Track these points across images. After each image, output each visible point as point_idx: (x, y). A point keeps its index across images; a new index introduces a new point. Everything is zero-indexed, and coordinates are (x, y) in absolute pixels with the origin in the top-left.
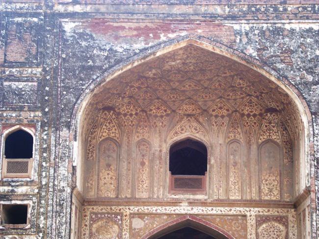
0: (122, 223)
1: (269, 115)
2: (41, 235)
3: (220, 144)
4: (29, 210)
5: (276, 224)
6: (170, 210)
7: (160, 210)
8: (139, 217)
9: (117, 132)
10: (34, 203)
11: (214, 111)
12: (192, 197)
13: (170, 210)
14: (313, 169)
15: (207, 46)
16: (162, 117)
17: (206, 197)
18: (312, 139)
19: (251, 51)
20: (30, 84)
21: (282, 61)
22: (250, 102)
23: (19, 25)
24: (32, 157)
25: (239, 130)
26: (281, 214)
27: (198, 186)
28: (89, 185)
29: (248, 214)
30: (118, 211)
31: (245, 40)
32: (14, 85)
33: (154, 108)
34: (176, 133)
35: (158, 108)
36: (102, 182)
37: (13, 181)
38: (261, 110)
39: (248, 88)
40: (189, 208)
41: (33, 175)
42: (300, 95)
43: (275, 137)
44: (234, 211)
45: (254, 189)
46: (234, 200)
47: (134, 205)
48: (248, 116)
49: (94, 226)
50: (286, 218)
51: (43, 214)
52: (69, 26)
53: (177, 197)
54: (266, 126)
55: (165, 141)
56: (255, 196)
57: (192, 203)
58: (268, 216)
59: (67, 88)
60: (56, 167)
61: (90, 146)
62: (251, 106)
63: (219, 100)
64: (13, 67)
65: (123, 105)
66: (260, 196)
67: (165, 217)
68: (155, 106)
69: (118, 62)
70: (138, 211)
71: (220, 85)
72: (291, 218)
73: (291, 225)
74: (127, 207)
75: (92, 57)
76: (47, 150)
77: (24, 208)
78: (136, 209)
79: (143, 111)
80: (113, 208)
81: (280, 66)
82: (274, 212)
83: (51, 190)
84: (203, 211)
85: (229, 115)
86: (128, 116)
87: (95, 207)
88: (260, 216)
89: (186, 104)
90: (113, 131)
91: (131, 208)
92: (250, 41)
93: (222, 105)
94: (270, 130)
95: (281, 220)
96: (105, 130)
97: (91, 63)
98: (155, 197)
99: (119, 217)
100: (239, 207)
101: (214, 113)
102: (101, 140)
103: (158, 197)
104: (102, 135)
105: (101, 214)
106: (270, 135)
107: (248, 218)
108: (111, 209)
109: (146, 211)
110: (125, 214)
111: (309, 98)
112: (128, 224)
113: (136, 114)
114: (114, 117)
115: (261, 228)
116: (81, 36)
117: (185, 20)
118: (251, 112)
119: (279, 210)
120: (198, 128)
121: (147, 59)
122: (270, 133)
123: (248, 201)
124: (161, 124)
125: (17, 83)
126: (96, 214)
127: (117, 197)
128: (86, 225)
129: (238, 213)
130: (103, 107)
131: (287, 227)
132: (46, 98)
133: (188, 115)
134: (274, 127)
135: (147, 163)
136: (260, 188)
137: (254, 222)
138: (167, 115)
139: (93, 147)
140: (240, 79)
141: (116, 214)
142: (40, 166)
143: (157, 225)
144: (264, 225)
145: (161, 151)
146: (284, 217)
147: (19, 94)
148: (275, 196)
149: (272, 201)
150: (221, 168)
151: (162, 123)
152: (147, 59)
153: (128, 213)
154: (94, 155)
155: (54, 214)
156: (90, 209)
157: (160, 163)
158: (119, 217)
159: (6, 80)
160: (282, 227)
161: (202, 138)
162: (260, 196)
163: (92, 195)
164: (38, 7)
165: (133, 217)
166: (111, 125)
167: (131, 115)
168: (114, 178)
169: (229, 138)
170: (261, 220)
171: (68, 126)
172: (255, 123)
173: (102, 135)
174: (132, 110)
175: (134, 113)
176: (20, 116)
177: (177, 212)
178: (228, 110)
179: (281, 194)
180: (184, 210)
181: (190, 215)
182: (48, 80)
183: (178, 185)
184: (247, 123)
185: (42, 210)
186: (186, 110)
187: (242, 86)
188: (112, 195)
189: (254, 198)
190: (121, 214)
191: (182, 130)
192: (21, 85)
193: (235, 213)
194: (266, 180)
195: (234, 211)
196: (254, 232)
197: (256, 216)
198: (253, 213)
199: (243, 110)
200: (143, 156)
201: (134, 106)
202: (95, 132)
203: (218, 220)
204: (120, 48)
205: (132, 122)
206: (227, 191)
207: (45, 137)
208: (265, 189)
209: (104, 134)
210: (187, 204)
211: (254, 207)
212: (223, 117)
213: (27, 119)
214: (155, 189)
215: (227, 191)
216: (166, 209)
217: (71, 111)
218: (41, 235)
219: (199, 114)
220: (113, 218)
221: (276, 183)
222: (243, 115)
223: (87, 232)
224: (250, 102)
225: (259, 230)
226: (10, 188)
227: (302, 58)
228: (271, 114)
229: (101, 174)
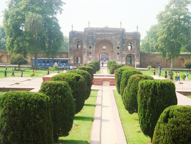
19: (110, 39)
52: (94, 37)
117: (104, 37)
130: (97, 43)
170: (110, 53)
204: (98, 39)
213: (91, 45)
217: (94, 44)
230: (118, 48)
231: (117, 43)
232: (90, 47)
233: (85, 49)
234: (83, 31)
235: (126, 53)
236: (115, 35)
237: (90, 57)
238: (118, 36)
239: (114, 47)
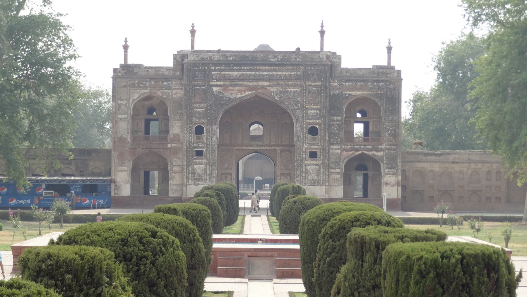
7: (246, 148)
15: (262, 96)
19: (276, 98)
21: (287, 102)
23: (198, 89)
31: (275, 94)
32: (197, 110)
42: (293, 113)
57: (258, 145)
60: (212, 138)
69: (232, 102)
75: (223, 100)
77: (202, 151)
81: (286, 103)
92: (276, 95)
116: (220, 92)
142: (207, 138)
147: (199, 113)
160: (289, 154)
164: (205, 83)
170: (282, 151)
171: (216, 124)
192: (200, 110)
230: (313, 131)
231: (310, 111)
232: (199, 130)
233: (177, 138)
234: (170, 63)
236: (298, 78)
238: (314, 85)
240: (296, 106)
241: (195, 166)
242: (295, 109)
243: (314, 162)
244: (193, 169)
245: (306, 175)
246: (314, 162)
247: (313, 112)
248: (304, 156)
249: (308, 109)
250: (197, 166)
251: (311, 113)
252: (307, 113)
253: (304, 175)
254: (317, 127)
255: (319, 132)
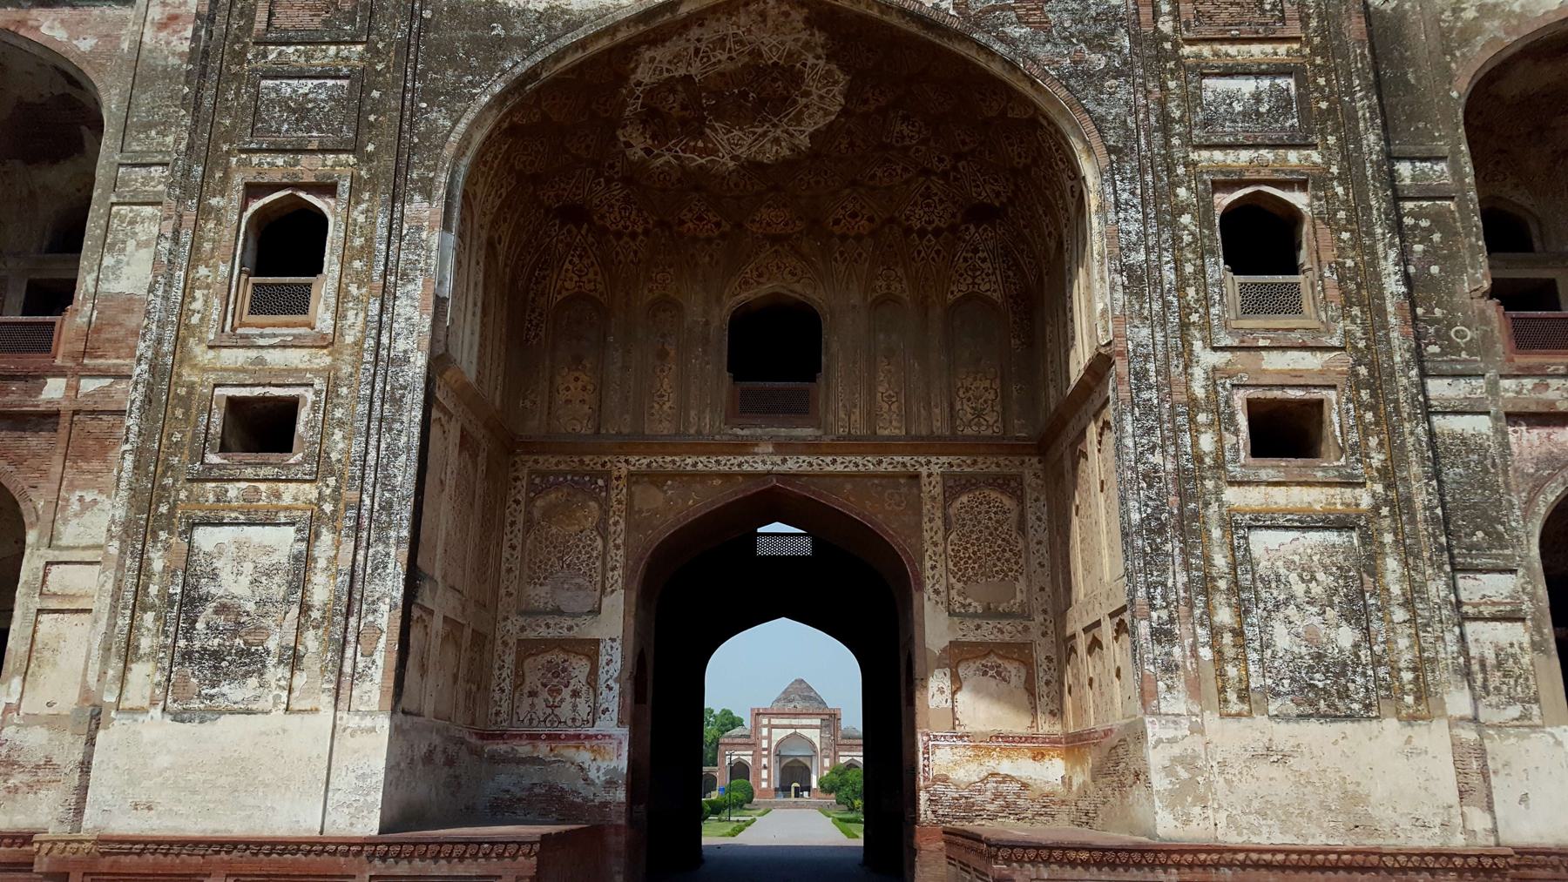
0: (608, 497)
1: (972, 229)
2: (332, 481)
3: (854, 307)
4: (304, 415)
5: (993, 495)
6: (730, 463)
7: (705, 463)
8: (652, 483)
9: (599, 278)
10: (317, 393)
11: (837, 222)
12: (783, 431)
13: (730, 463)
14: (1119, 295)
16: (709, 240)
17: (819, 433)
18: (1111, 216)
20: (330, 83)
22: (927, 194)
24: (320, 271)
25: (900, 271)
26: (1006, 470)
27: (800, 409)
28: (528, 404)
29: (924, 471)
30: (599, 467)
33: (690, 215)
34: (746, 283)
35: (700, 219)
36: (562, 396)
37: (262, 336)
38: (954, 215)
39: (923, 148)
40: (778, 459)
41: (322, 315)
43: (987, 286)
44: (888, 464)
45: (937, 411)
46: (889, 438)
47: (638, 454)
48: (922, 233)
49: (539, 503)
50: (1019, 478)
51: (341, 423)
53: (746, 432)
54: (965, 260)
55: (719, 300)
56: (940, 426)
57: (784, 447)
58: (972, 475)
59: (431, 95)
61: (533, 311)
62: (928, 205)
63: (847, 191)
64: (288, 44)
65: (612, 206)
66: (953, 428)
67: (717, 482)
68: (690, 210)
70: (649, 465)
71: (852, 144)
72: (1029, 478)
73: (1030, 495)
74: (622, 458)
76: (367, 251)
78: (645, 461)
79: (662, 224)
80: (587, 459)
81: (1016, 32)
82: (987, 465)
83: (368, 357)
84: (810, 464)
85: (873, 234)
86: (626, 239)
87: (541, 459)
88: (953, 475)
89: (769, 206)
90: (591, 276)
91: (632, 459)
93: (858, 207)
94: (975, 269)
95: (1008, 484)
96: (570, 274)
97: (499, 30)
98: (692, 431)
99: (600, 482)
100: (902, 454)
101: (837, 230)
102: (559, 298)
103: (699, 432)
104: (563, 287)
105: (557, 474)
106: (974, 283)
107: (925, 480)
108: (582, 462)
109: (670, 467)
110: (616, 474)
111: (1101, 110)
112: (622, 497)
113: (646, 232)
114: (590, 239)
115: (957, 504)
118: (930, 222)
119: (1001, 459)
120: (799, 271)
121: (660, 21)
122: (974, 277)
123: (923, 438)
124: (707, 259)
125: (295, 82)
126: (543, 475)
127: (597, 432)
128: (517, 502)
129: (899, 469)
131: (1021, 500)
132: (372, 118)
133: (776, 239)
134: (984, 260)
135: (672, 353)
136: (952, 406)
137: (939, 489)
138: (723, 236)
139: (541, 314)
140: (905, 118)
141: (595, 475)
142: (341, 294)
143: (695, 502)
144: (964, 499)
145: (707, 323)
146: (1013, 477)
147: (301, 111)
148: (990, 425)
149: (985, 437)
150: (855, 363)
151: (711, 256)
152: (654, 24)
153: (624, 472)
154: (542, 334)
155: (374, 425)
156: (527, 465)
157: (705, 352)
158: (600, 482)
159: (265, 77)
160: (1008, 503)
161: (809, 292)
162: (953, 428)
163: (533, 427)
165: (636, 483)
166: (585, 262)
167: (634, 236)
168: (590, 387)
169: (874, 290)
170: (955, 485)
172: (938, 252)
173: (563, 287)
174: (634, 223)
175: (640, 230)
176: (297, 163)
177: (745, 467)
178: (871, 219)
179: (1004, 420)
180: (764, 462)
181: (779, 475)
182: (379, 73)
183: (747, 408)
184: (919, 252)
185: (338, 413)
186: (768, 224)
187: (907, 142)
188: (584, 428)
189: (937, 432)
190: (607, 476)
191: (760, 275)
193: (890, 469)
194: (967, 390)
195: (888, 464)
196: (939, 514)
197: (943, 474)
198: (936, 469)
199: (908, 219)
200: (663, 336)
201: (640, 211)
202: (544, 278)
203: (849, 486)
205: (636, 252)
206: (872, 416)
207: (361, 219)
208: (965, 410)
209: (567, 284)
210: (771, 449)
211: (938, 454)
212: (859, 238)
214: (693, 413)
215: (872, 416)
216: (718, 462)
218: (332, 481)
219: (801, 232)
220: (589, 484)
221: (992, 396)
222: (908, 231)
223: (520, 519)
224: (927, 194)
225: (951, 511)
226: (253, 353)
227: (1073, 12)
228: (977, 228)
229: (559, 379)
235: (1527, 440)
237: (234, 584)
239: (1108, 212)
240: (1098, 43)
241: (206, 538)
242: (1091, 78)
243: (1314, 498)
244: (189, 566)
245: (1242, 612)
246: (1314, 498)
247: (1247, 86)
248: (1207, 442)
249: (1203, 71)
250: (225, 534)
251: (1231, 97)
252: (1192, 99)
253: (1224, 616)
254: (1299, 199)
255: (1314, 246)
